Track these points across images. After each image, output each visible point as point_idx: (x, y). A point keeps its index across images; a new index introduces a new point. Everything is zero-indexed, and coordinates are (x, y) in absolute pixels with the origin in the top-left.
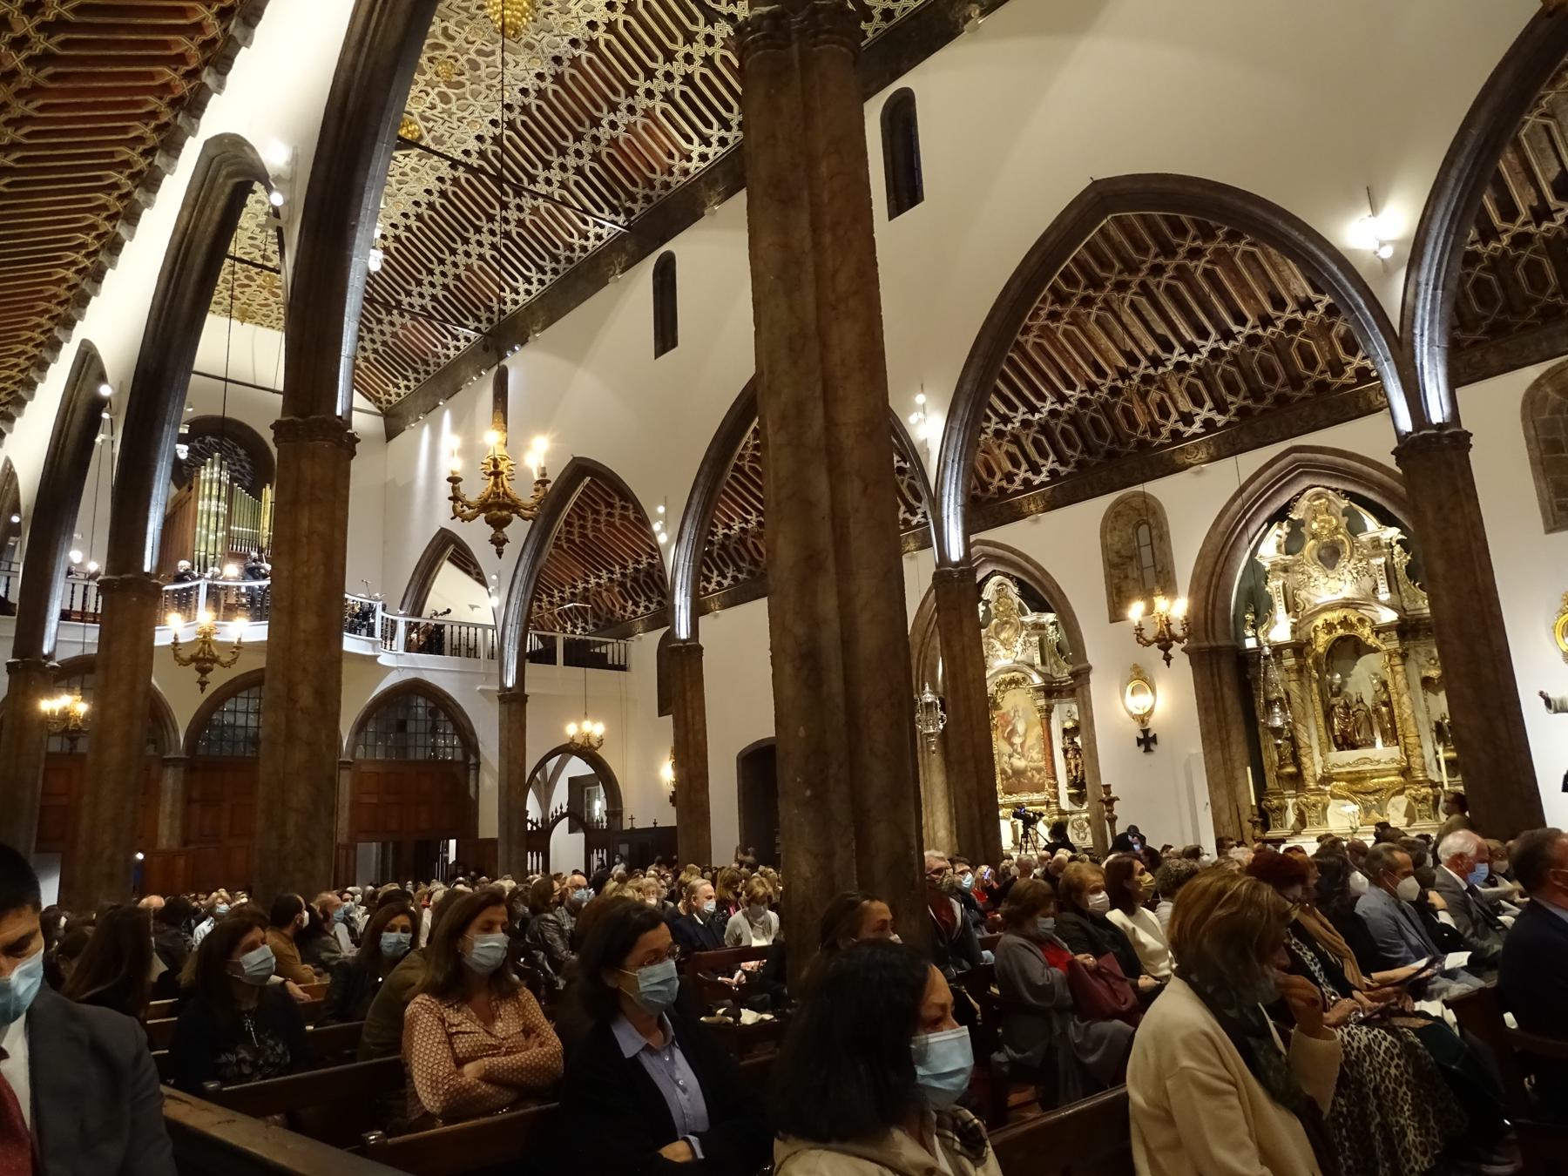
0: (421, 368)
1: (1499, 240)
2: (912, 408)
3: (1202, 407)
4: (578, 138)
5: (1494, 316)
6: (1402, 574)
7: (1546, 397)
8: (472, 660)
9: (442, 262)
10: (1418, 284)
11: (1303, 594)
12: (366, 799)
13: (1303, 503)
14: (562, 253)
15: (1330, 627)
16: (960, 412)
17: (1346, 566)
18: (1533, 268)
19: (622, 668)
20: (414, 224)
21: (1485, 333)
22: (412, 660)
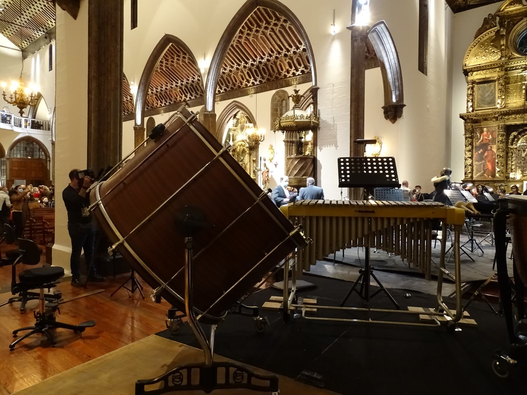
0: (30, 39)
2: (132, 85)
5: (267, 77)
8: (47, 131)
12: (14, 168)
15: (240, 146)
16: (141, 87)
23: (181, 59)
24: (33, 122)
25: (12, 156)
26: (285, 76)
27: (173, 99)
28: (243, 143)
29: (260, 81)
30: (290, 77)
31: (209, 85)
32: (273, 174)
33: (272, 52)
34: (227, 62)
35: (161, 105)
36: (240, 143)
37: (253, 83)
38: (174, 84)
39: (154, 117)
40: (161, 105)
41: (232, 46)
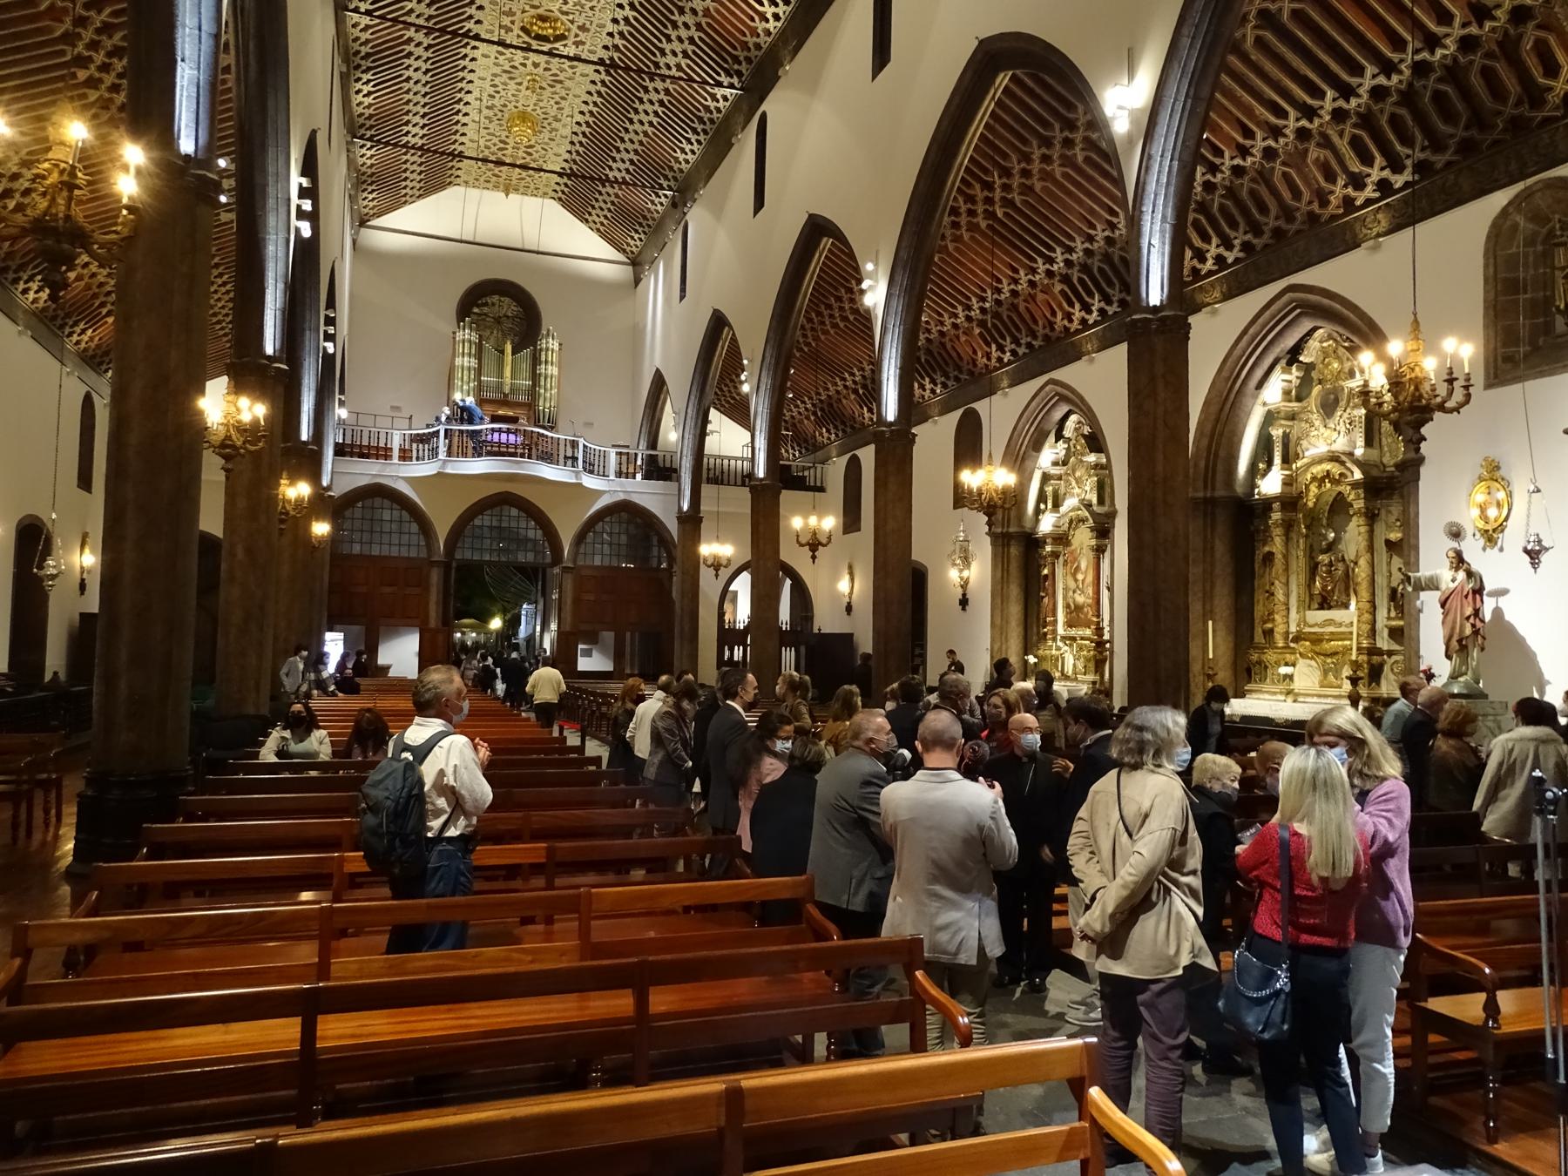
1: (1445, 47)
3: (1209, 243)
5: (1461, 133)
7: (1515, 226)
9: (627, 130)
11: (1304, 443)
13: (1313, 344)
14: (706, 116)
15: (1321, 481)
16: (898, 278)
17: (1340, 417)
18: (1488, 74)
19: (822, 489)
20: (599, 100)
21: (1456, 152)
22: (621, 485)
24: (651, 461)
27: (1040, 331)
28: (1335, 469)
29: (1420, 167)
31: (1151, 187)
32: (1503, 602)
34: (1249, 112)
38: (1041, 267)
39: (975, 405)
40: (1000, 360)
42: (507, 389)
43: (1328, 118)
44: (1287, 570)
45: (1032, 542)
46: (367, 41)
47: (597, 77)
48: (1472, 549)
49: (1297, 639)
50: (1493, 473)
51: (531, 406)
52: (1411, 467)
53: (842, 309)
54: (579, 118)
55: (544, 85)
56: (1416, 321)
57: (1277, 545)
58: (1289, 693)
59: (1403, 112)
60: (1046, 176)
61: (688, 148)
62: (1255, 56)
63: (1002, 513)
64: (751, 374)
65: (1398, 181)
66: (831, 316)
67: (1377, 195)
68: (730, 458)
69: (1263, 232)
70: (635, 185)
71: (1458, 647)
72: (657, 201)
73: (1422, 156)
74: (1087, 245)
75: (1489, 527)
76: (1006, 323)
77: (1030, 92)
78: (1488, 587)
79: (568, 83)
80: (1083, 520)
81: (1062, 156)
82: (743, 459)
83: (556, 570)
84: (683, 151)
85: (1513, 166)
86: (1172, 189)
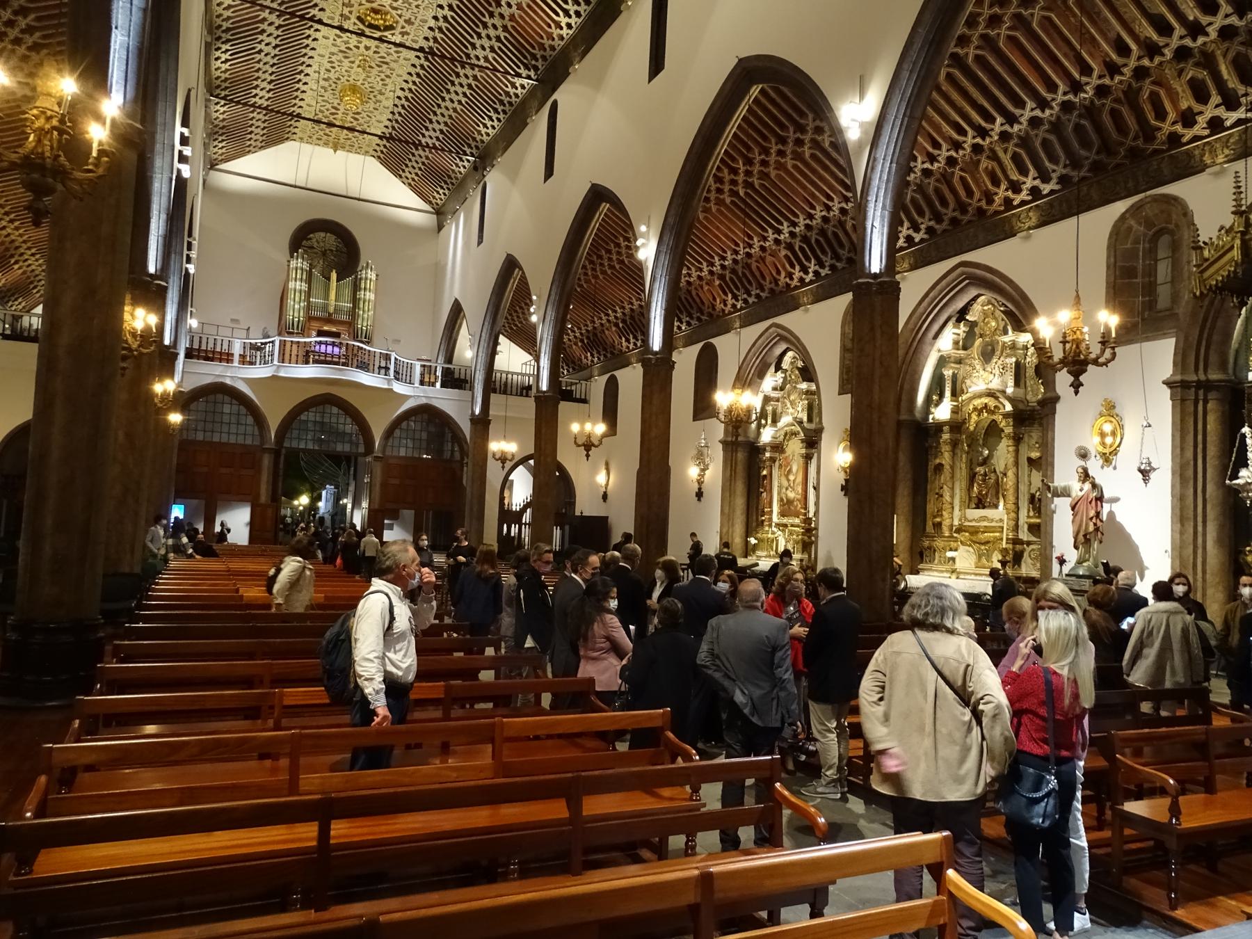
4: (491, 15)
5: (1093, 156)
6: (1030, 372)
7: (1130, 228)
9: (439, 106)
10: (875, 159)
11: (968, 382)
13: (977, 307)
14: (506, 100)
15: (979, 411)
16: (666, 239)
18: (1115, 114)
19: (584, 401)
20: (417, 80)
21: (1089, 171)
22: (424, 391)
23: (789, 148)
25: (388, 453)
26: (1174, 139)
27: (767, 285)
28: (992, 403)
29: (1063, 180)
30: (1196, 138)
31: (875, 182)
33: (1123, 50)
34: (938, 129)
35: (734, 306)
36: (978, 402)
37: (1035, 192)
38: (771, 235)
40: (734, 306)
41: (957, 60)
42: (331, 310)
43: (996, 138)
44: (952, 477)
45: (754, 450)
46: (229, 18)
47: (417, 62)
48: (1094, 466)
49: (959, 531)
50: (1110, 410)
51: (351, 324)
52: (1050, 403)
53: (610, 259)
54: (400, 93)
55: (373, 64)
56: (1078, 296)
57: (946, 458)
58: (953, 571)
59: (1052, 138)
60: (780, 166)
61: (489, 123)
62: (945, 87)
63: (737, 422)
64: (538, 307)
65: (1046, 189)
66: (602, 265)
67: (1030, 198)
68: (513, 374)
69: (949, 219)
70: (443, 150)
71: (1084, 540)
72: (460, 164)
73: (1064, 172)
74: (808, 221)
75: (1107, 451)
76: (741, 278)
77: (772, 101)
78: (1106, 495)
79: (393, 65)
80: (795, 434)
81: (793, 152)
82: (529, 376)
83: (369, 459)
84: (485, 126)
85: (1130, 184)
86: (891, 185)
